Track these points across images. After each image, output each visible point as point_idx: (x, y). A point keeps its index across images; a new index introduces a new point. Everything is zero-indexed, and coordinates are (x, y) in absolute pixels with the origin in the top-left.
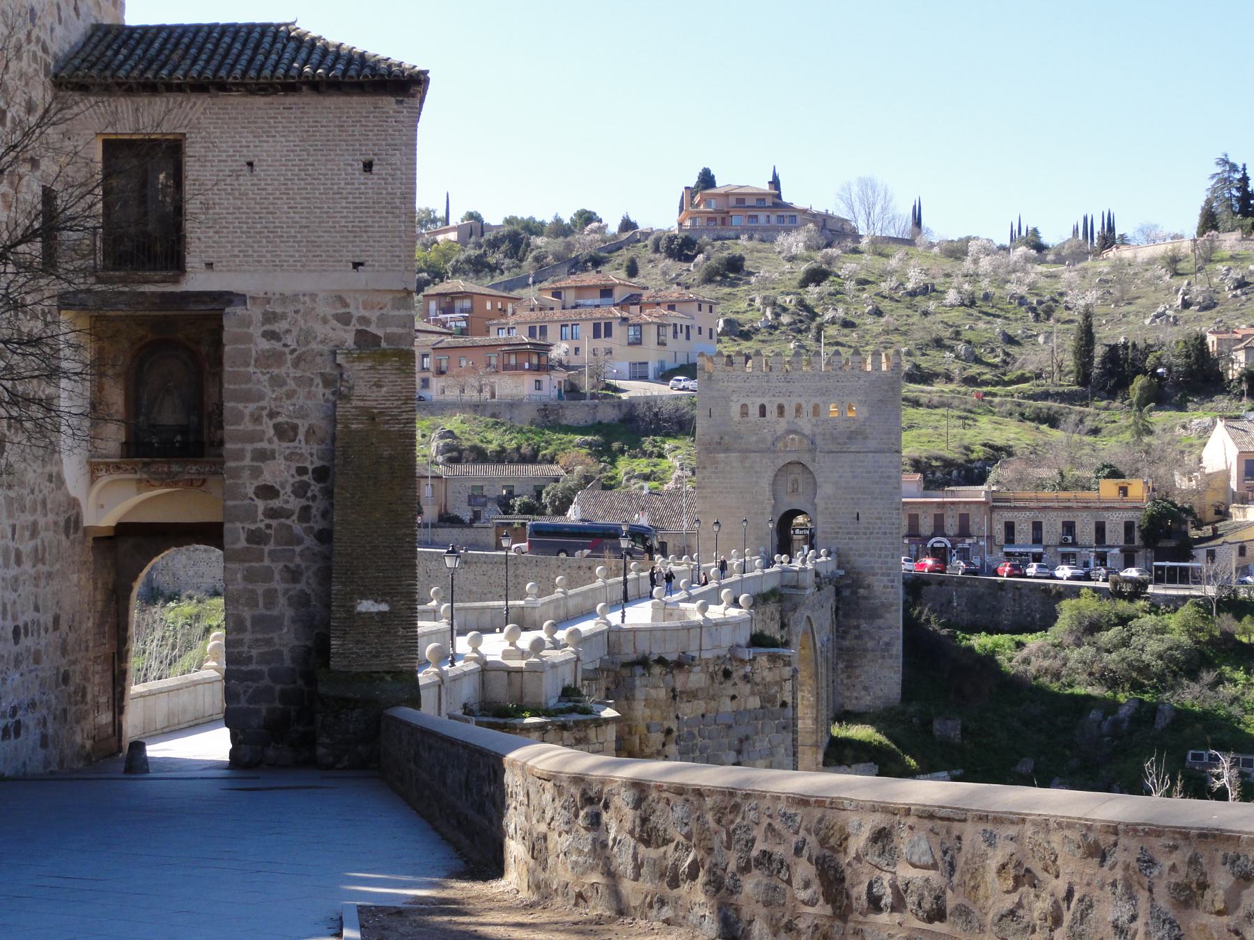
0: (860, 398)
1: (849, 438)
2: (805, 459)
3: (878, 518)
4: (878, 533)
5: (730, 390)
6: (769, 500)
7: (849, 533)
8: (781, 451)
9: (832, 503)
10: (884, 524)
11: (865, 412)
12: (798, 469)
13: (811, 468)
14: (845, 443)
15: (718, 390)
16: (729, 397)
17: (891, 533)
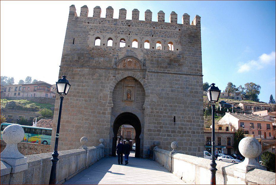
0: (176, 39)
1: (169, 64)
2: (138, 75)
3: (187, 121)
4: (189, 132)
5: (89, 27)
6: (110, 103)
7: (167, 131)
8: (121, 69)
9: (156, 109)
10: (194, 125)
11: (179, 47)
12: (132, 84)
13: (142, 83)
14: (166, 68)
15: (81, 27)
16: (88, 32)
17: (198, 133)
